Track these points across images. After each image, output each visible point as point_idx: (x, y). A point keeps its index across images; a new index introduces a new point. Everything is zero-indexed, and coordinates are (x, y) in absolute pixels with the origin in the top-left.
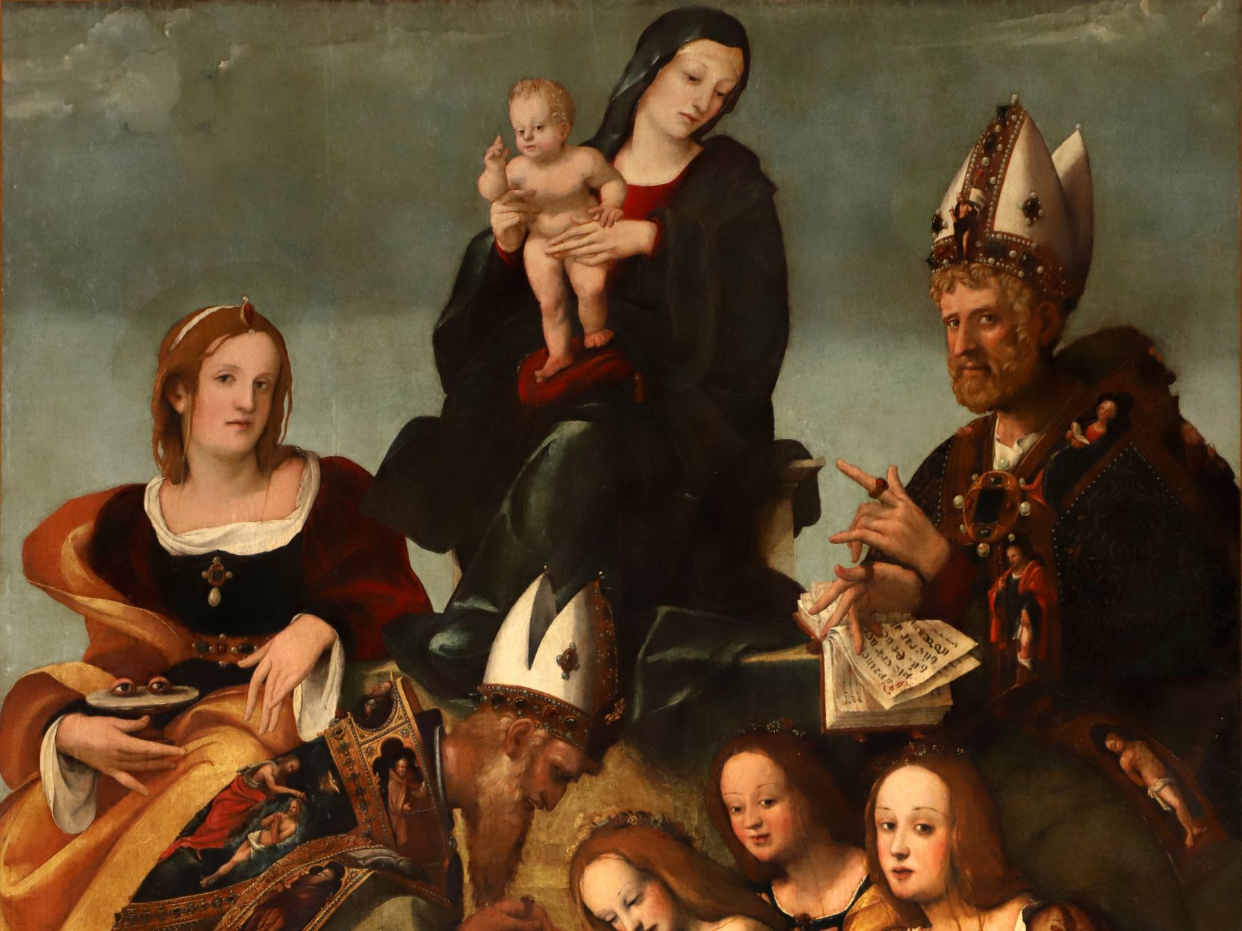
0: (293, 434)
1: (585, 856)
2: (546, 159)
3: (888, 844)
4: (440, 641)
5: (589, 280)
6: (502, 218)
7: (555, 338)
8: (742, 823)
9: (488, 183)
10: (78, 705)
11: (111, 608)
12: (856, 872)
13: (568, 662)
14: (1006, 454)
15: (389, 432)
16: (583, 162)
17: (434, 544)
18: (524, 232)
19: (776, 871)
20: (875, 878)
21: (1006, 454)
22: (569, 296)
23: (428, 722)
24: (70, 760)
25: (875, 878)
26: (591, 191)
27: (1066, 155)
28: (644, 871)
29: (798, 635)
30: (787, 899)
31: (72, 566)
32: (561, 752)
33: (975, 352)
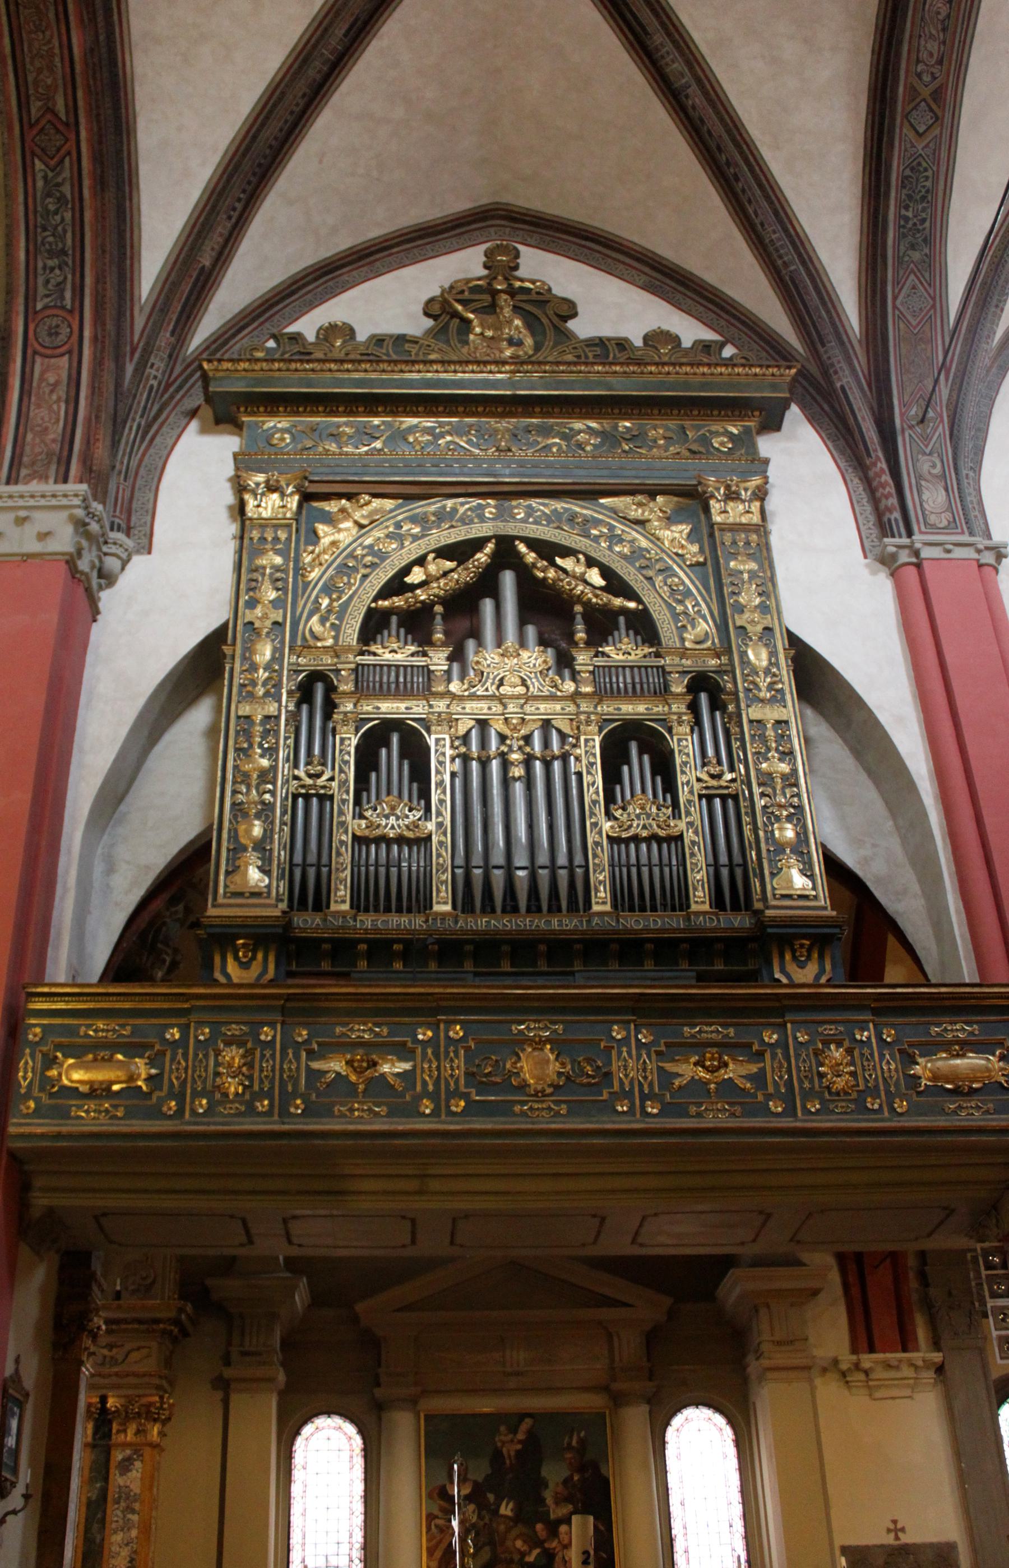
0: (470, 1476)
1: (515, 1540)
2: (505, 1435)
3: (561, 1536)
4: (493, 1507)
5: (512, 1453)
6: (499, 1444)
7: (508, 1462)
8: (539, 1534)
9: (497, 1439)
10: (436, 1517)
11: (442, 1503)
12: (556, 1541)
13: (512, 1510)
14: (576, 1478)
15: (483, 1475)
16: (511, 1436)
17: (490, 1492)
18: (502, 1447)
19: (544, 1541)
20: (559, 1542)
21: (576, 1478)
22: (509, 1456)
23: (491, 1520)
24: (437, 1526)
25: (559, 1542)
26: (512, 1441)
27: (582, 1434)
28: (525, 1542)
29: (545, 1505)
30: (546, 1545)
31: (435, 1495)
32: (511, 1524)
33: (570, 1463)
